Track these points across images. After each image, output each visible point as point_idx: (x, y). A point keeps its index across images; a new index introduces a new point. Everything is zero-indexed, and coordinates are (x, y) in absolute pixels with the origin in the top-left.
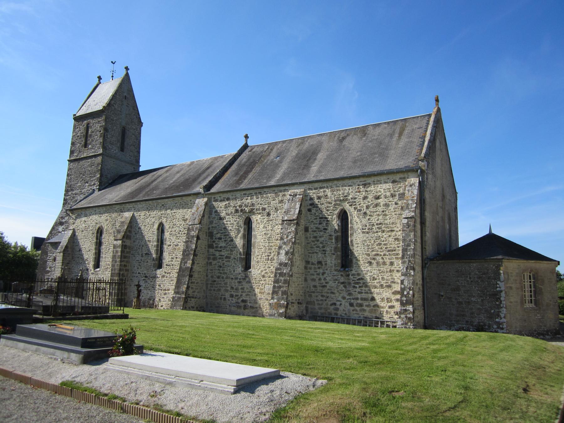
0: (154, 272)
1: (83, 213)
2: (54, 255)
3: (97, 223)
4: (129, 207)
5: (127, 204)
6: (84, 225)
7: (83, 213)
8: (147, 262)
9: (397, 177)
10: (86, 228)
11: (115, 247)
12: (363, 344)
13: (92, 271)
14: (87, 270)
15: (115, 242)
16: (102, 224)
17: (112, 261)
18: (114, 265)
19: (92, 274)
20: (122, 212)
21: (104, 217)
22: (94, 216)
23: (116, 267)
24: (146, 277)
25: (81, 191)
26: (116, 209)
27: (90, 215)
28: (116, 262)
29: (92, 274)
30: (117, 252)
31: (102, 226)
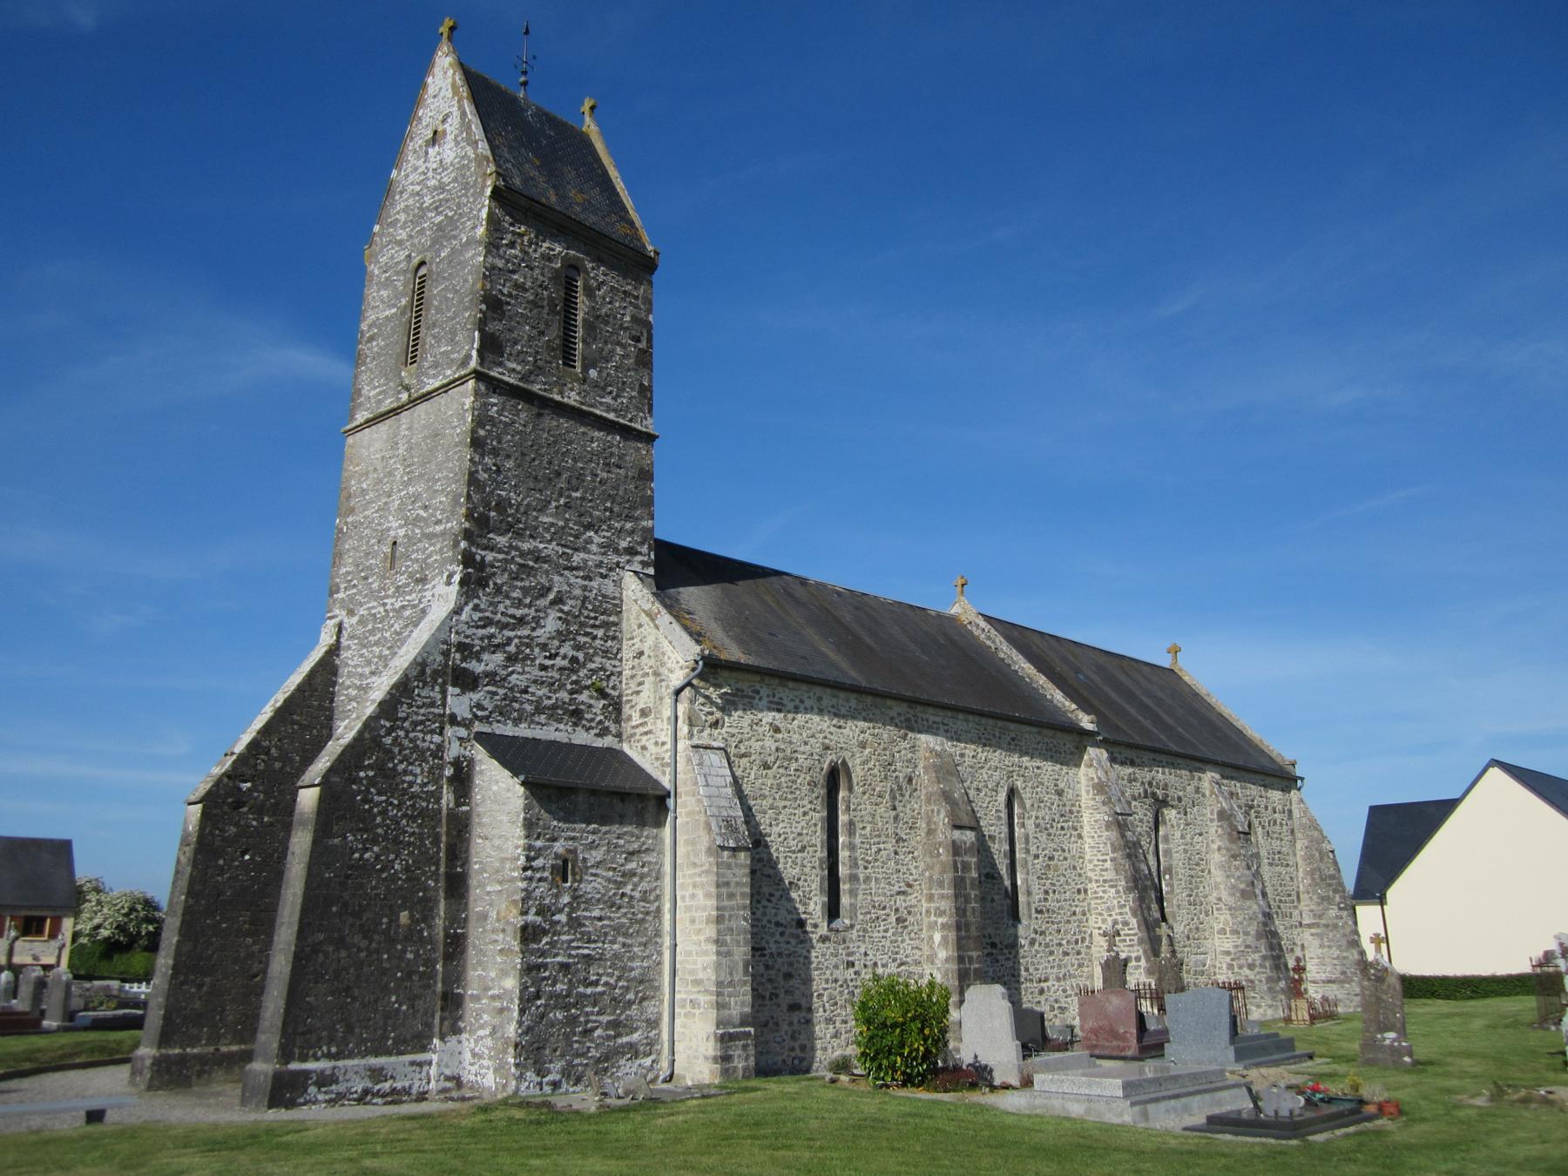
0: (1011, 931)
1: (764, 691)
2: (559, 847)
3: (827, 748)
4: (932, 718)
5: (931, 710)
6: (770, 744)
7: (764, 691)
8: (993, 900)
9: (1228, 771)
10: (786, 757)
11: (956, 849)
12: (212, 1118)
13: (823, 929)
14: (801, 924)
15: (957, 834)
16: (847, 755)
17: (956, 896)
18: (965, 911)
19: (824, 939)
20: (912, 730)
21: (854, 730)
22: (816, 718)
23: (971, 919)
24: (993, 945)
25: (569, 557)
26: (893, 713)
27: (796, 710)
28: (967, 900)
29: (824, 939)
30: (966, 867)
31: (844, 763)
